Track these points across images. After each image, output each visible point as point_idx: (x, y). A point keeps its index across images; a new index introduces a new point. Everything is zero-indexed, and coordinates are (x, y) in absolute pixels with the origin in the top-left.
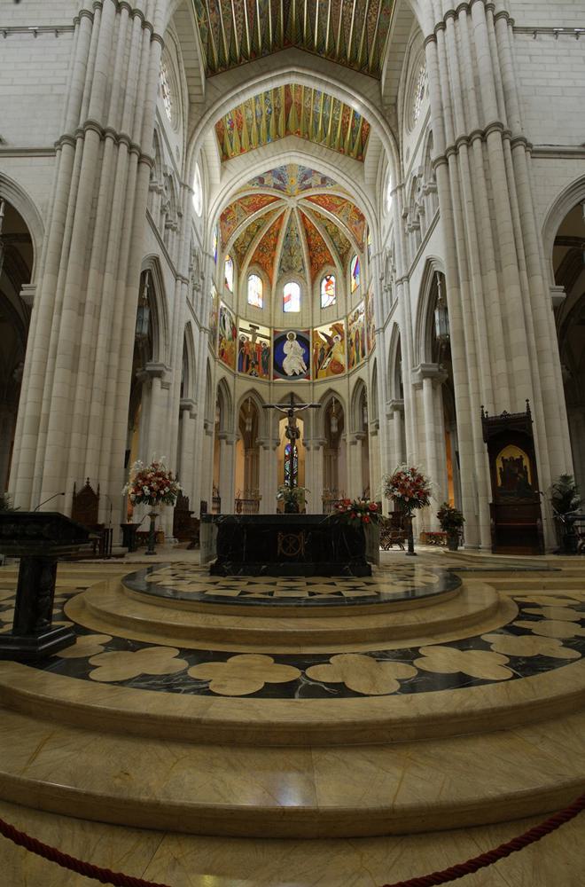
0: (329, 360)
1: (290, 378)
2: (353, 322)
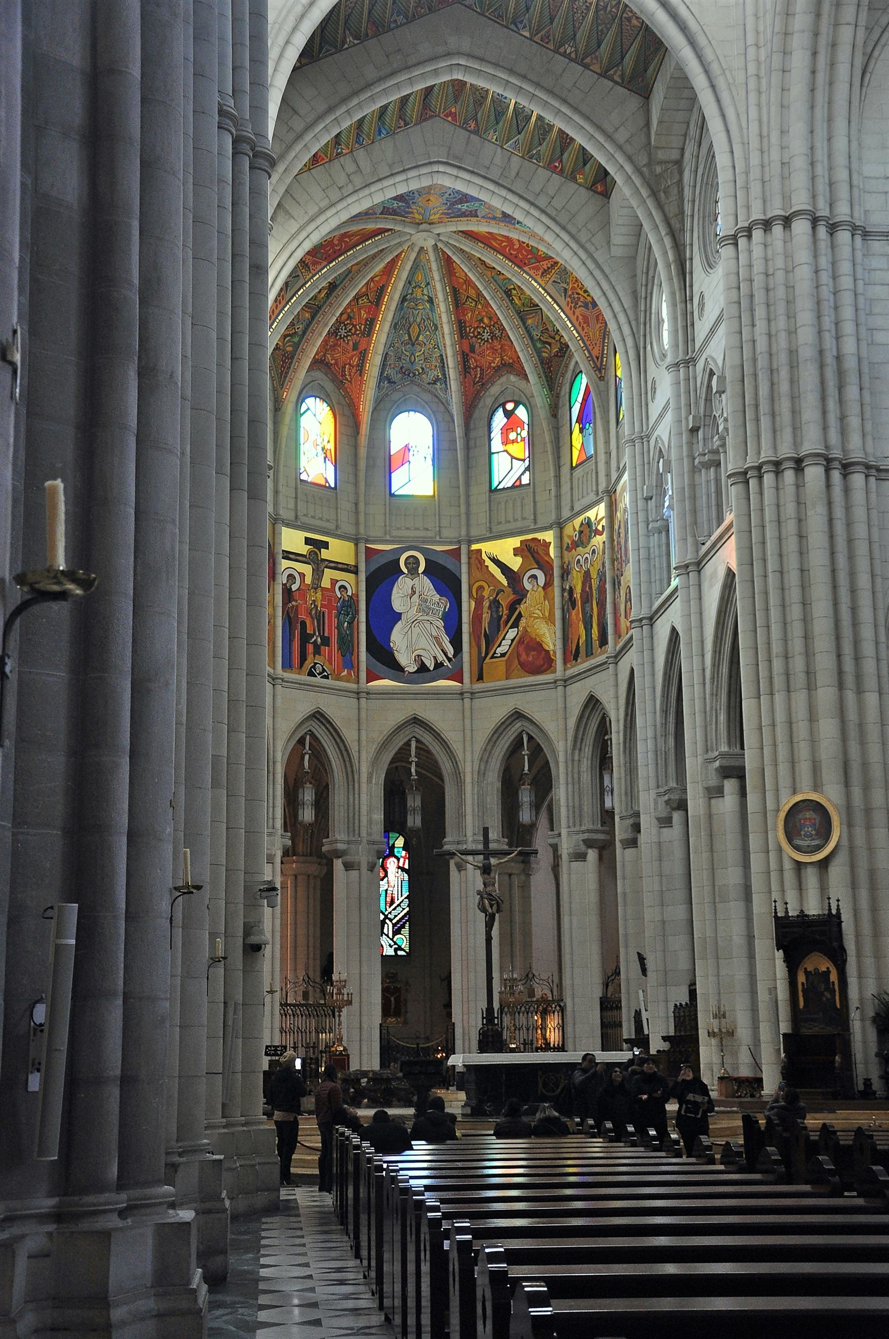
0: (512, 633)
1: (410, 679)
2: (575, 545)
